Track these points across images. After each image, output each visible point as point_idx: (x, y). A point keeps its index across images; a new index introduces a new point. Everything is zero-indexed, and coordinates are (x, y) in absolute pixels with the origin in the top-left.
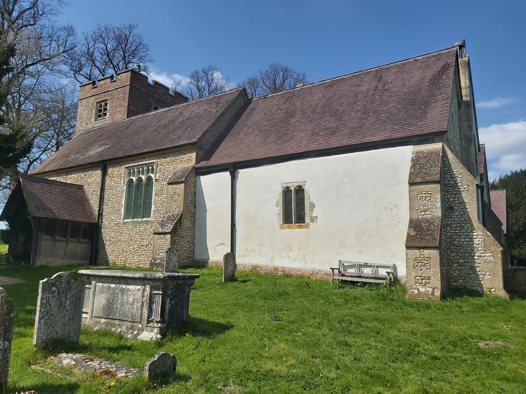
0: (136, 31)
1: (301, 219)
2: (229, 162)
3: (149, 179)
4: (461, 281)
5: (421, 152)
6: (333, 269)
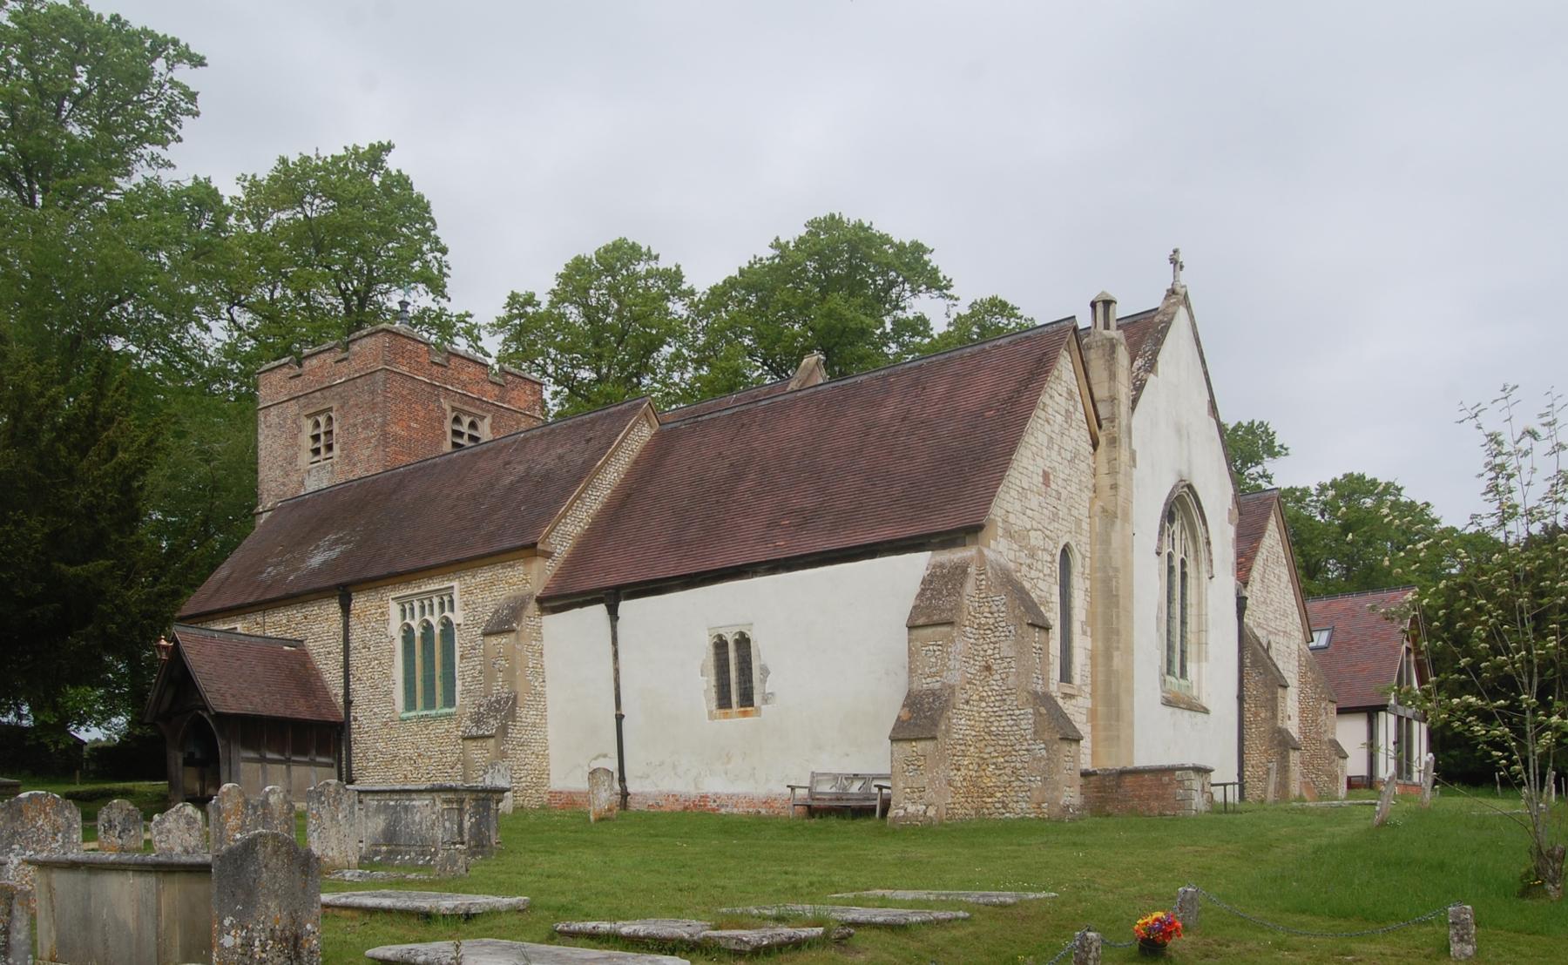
1: (747, 699)
2: (603, 584)
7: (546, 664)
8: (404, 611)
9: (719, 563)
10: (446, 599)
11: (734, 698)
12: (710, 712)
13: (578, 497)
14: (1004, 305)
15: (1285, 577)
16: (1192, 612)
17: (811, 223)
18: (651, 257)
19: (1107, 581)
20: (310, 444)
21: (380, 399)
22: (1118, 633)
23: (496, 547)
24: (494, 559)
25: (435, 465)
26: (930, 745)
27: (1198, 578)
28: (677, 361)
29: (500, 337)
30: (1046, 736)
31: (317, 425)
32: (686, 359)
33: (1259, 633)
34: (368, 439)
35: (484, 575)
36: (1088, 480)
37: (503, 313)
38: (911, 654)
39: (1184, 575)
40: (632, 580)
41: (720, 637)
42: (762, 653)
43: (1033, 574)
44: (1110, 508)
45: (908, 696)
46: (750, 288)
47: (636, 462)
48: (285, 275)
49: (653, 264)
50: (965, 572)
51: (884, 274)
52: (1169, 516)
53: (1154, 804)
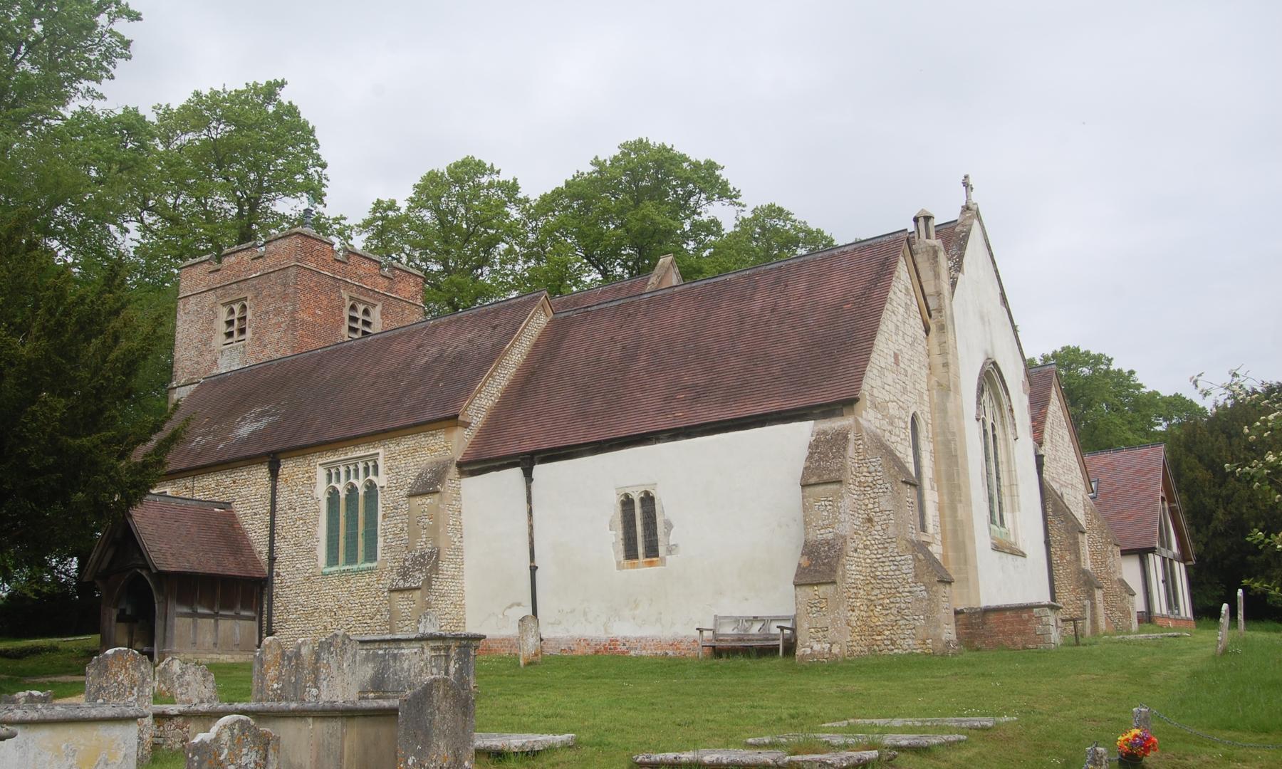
0: (285, 96)
1: (652, 551)
3: (371, 487)
4: (887, 633)
5: (825, 433)
6: (701, 630)
7: (463, 522)
8: (330, 475)
9: (624, 431)
10: (371, 464)
11: (641, 550)
12: (618, 563)
13: (490, 375)
14: (781, 210)
15: (1067, 438)
16: (1003, 468)
17: (624, 146)
18: (492, 170)
19: (947, 443)
20: (224, 328)
21: (291, 290)
22: (959, 487)
23: (420, 419)
24: (418, 429)
25: (351, 347)
26: (830, 588)
27: (1006, 440)
28: (510, 256)
29: (365, 236)
30: (926, 579)
31: (232, 312)
32: (517, 254)
33: (1055, 486)
34: (279, 324)
35: (408, 443)
36: (923, 359)
37: (368, 216)
38: (805, 509)
39: (994, 436)
40: (545, 446)
41: (627, 495)
42: (666, 509)
43: (893, 439)
44: (943, 382)
45: (805, 545)
46: (574, 197)
47: (536, 345)
48: (188, 186)
49: (494, 177)
50: (846, 438)
51: (683, 186)
52: (981, 391)
53: (1017, 639)
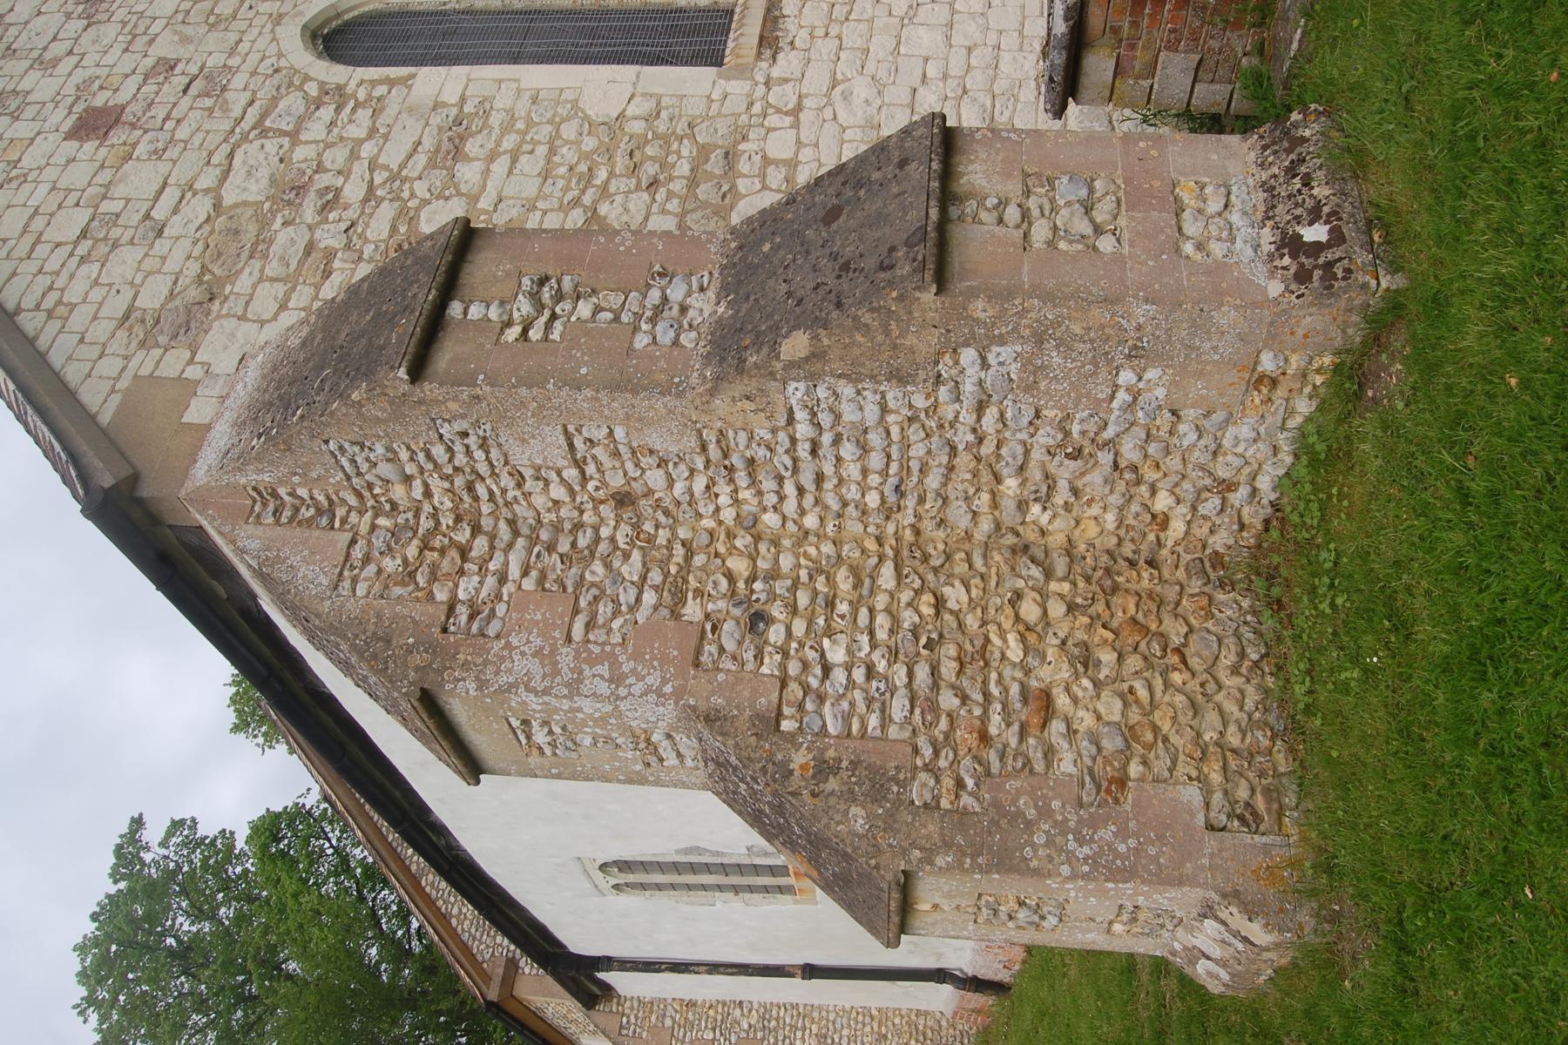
30: (922, 342)
